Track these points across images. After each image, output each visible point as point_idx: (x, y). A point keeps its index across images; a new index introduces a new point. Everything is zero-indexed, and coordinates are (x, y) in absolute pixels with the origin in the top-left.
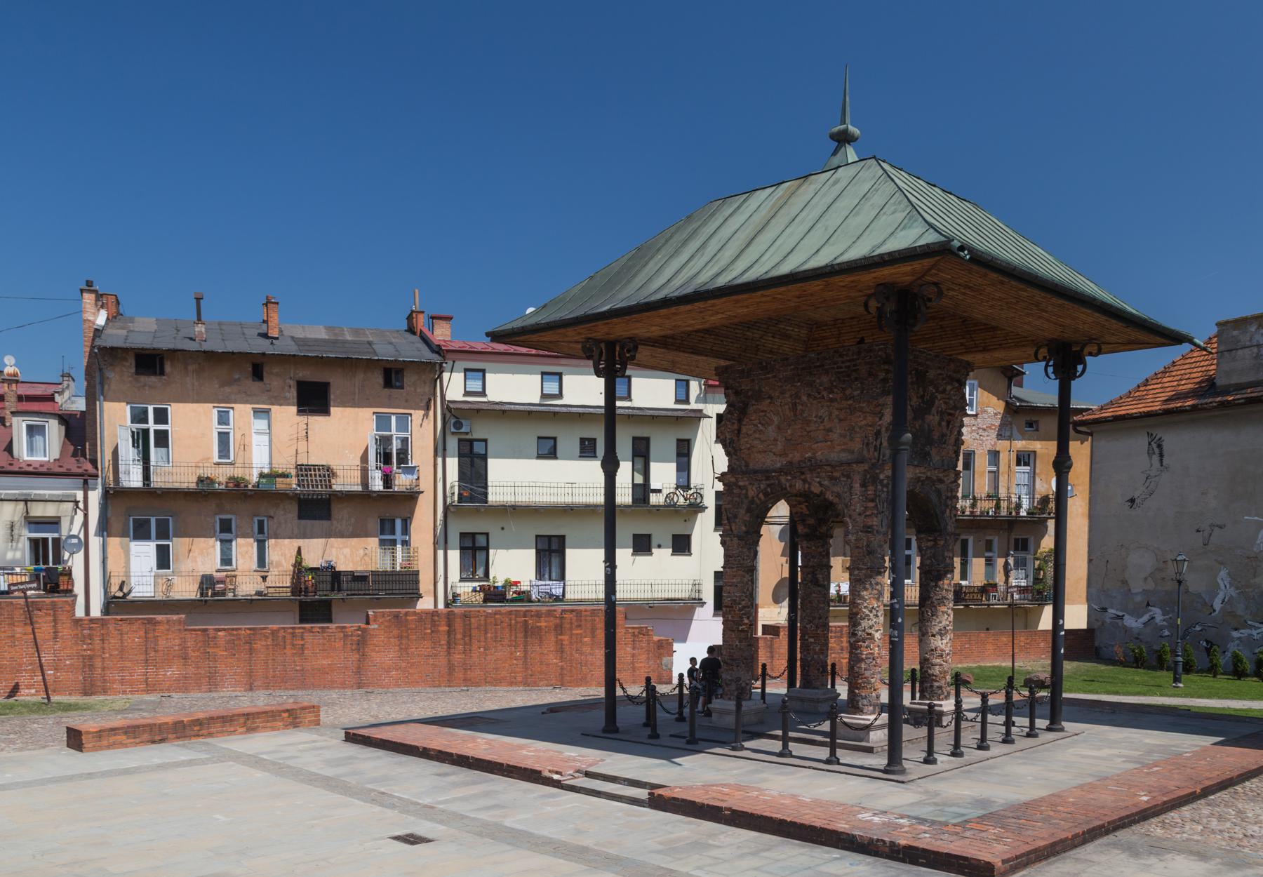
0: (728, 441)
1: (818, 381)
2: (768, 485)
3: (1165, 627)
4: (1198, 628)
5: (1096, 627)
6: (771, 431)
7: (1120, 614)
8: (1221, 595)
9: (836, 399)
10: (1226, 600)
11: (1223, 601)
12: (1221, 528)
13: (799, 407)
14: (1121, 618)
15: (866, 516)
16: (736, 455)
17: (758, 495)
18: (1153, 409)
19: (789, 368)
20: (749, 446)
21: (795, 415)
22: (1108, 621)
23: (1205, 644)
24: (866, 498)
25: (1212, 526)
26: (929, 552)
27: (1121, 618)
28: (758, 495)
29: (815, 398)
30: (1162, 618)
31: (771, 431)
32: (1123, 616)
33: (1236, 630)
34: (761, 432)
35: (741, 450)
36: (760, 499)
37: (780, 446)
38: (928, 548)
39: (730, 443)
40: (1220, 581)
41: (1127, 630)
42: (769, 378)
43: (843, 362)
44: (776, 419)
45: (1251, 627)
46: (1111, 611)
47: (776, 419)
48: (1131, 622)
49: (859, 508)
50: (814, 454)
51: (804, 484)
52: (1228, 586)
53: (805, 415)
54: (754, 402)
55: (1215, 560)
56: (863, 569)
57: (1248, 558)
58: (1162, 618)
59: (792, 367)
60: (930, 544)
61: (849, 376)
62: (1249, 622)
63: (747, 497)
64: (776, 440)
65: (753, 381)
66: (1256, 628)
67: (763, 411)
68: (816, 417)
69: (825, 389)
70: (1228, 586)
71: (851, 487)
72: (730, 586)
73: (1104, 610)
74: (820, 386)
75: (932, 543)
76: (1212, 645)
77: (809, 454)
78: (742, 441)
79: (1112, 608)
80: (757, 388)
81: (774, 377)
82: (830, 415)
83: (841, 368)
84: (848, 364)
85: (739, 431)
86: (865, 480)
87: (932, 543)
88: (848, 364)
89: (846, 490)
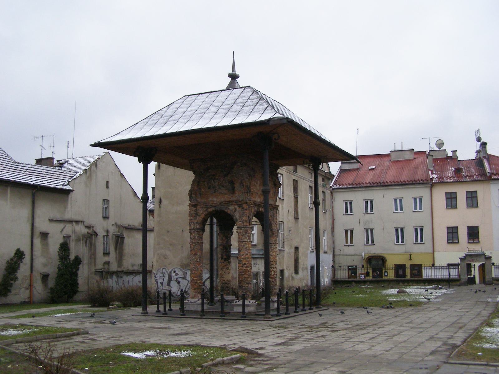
0: (248, 187)
28: (254, 212)
35: (251, 191)
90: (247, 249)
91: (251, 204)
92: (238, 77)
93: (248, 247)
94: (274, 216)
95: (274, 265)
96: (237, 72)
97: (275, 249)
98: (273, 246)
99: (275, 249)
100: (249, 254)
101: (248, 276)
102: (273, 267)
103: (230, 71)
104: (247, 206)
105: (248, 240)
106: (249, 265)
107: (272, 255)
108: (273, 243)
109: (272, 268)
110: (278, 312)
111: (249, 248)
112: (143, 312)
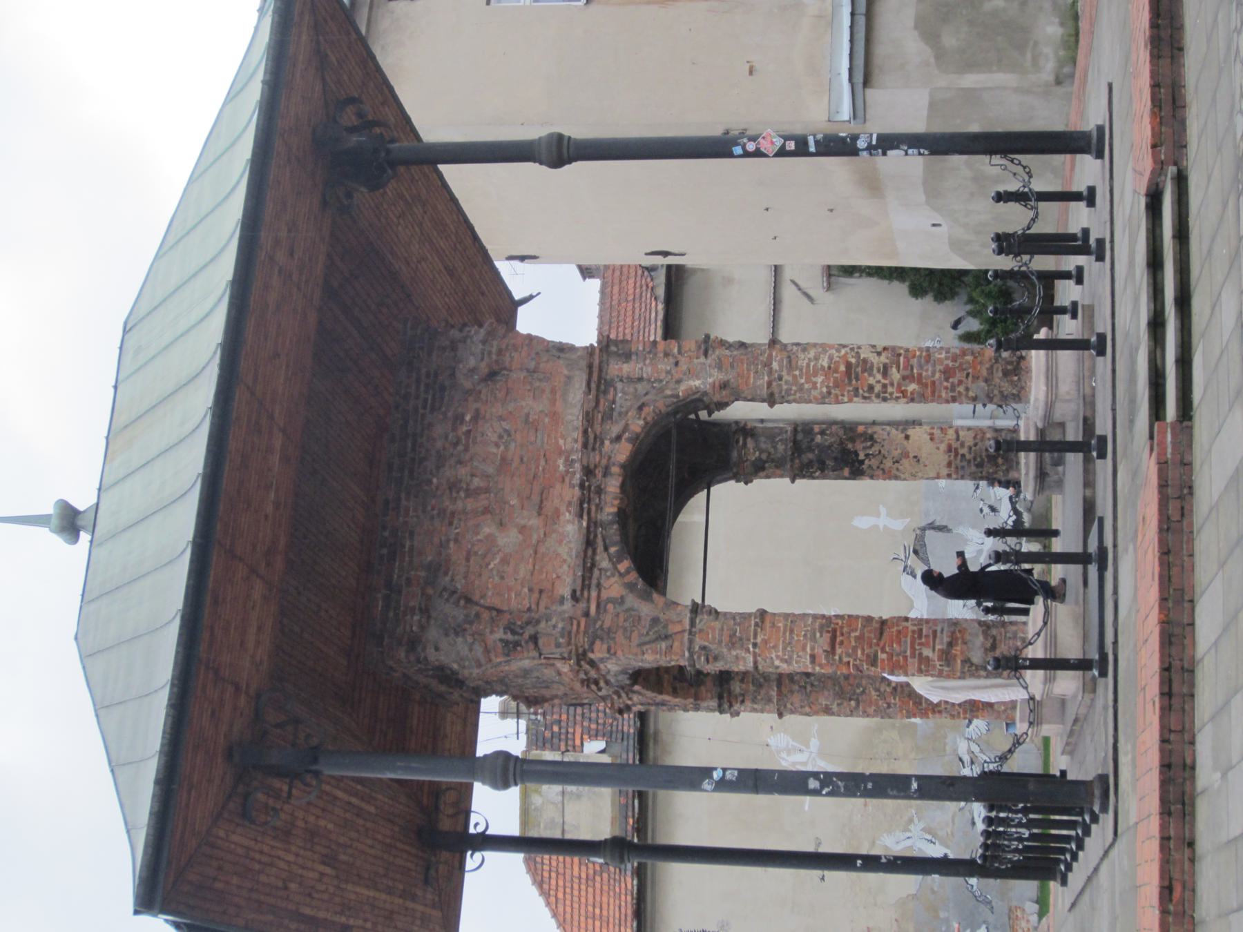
0: (510, 637)
1: (439, 444)
2: (606, 549)
6: (508, 539)
9: (477, 411)
10: (929, 837)
11: (932, 842)
12: (820, 843)
13: (477, 482)
15: (680, 352)
16: (538, 622)
17: (621, 575)
19: (404, 503)
20: (526, 590)
21: (487, 490)
24: (649, 352)
26: (763, 446)
29: (466, 449)
31: (508, 539)
34: (505, 561)
35: (529, 609)
36: (628, 572)
37: (534, 522)
38: (757, 448)
39: (514, 633)
42: (412, 548)
43: (417, 397)
44: (486, 530)
47: (486, 530)
50: (560, 452)
51: (611, 474)
52: (909, 834)
53: (491, 470)
54: (448, 579)
56: (770, 356)
59: (403, 495)
60: (750, 443)
61: (443, 389)
63: (622, 600)
64: (522, 529)
65: (409, 582)
67: (468, 560)
68: (497, 445)
69: (454, 429)
70: (909, 834)
71: (630, 380)
72: (792, 631)
74: (446, 437)
75: (749, 440)
77: (561, 462)
78: (514, 604)
80: (422, 574)
81: (412, 534)
82: (501, 418)
83: (426, 400)
84: (422, 388)
85: (490, 609)
86: (619, 355)
87: (749, 440)
88: (422, 388)
89: (631, 390)
90: (791, 658)
91: (587, 614)
93: (780, 654)
94: (640, 379)
95: (871, 381)
96: (49, 509)
97: (797, 373)
98: (783, 383)
99: (797, 373)
100: (813, 649)
101: (913, 656)
102: (885, 386)
104: (598, 643)
105: (748, 650)
106: (863, 650)
107: (825, 390)
108: (769, 384)
109: (890, 389)
111: (784, 649)
112: (1059, 880)
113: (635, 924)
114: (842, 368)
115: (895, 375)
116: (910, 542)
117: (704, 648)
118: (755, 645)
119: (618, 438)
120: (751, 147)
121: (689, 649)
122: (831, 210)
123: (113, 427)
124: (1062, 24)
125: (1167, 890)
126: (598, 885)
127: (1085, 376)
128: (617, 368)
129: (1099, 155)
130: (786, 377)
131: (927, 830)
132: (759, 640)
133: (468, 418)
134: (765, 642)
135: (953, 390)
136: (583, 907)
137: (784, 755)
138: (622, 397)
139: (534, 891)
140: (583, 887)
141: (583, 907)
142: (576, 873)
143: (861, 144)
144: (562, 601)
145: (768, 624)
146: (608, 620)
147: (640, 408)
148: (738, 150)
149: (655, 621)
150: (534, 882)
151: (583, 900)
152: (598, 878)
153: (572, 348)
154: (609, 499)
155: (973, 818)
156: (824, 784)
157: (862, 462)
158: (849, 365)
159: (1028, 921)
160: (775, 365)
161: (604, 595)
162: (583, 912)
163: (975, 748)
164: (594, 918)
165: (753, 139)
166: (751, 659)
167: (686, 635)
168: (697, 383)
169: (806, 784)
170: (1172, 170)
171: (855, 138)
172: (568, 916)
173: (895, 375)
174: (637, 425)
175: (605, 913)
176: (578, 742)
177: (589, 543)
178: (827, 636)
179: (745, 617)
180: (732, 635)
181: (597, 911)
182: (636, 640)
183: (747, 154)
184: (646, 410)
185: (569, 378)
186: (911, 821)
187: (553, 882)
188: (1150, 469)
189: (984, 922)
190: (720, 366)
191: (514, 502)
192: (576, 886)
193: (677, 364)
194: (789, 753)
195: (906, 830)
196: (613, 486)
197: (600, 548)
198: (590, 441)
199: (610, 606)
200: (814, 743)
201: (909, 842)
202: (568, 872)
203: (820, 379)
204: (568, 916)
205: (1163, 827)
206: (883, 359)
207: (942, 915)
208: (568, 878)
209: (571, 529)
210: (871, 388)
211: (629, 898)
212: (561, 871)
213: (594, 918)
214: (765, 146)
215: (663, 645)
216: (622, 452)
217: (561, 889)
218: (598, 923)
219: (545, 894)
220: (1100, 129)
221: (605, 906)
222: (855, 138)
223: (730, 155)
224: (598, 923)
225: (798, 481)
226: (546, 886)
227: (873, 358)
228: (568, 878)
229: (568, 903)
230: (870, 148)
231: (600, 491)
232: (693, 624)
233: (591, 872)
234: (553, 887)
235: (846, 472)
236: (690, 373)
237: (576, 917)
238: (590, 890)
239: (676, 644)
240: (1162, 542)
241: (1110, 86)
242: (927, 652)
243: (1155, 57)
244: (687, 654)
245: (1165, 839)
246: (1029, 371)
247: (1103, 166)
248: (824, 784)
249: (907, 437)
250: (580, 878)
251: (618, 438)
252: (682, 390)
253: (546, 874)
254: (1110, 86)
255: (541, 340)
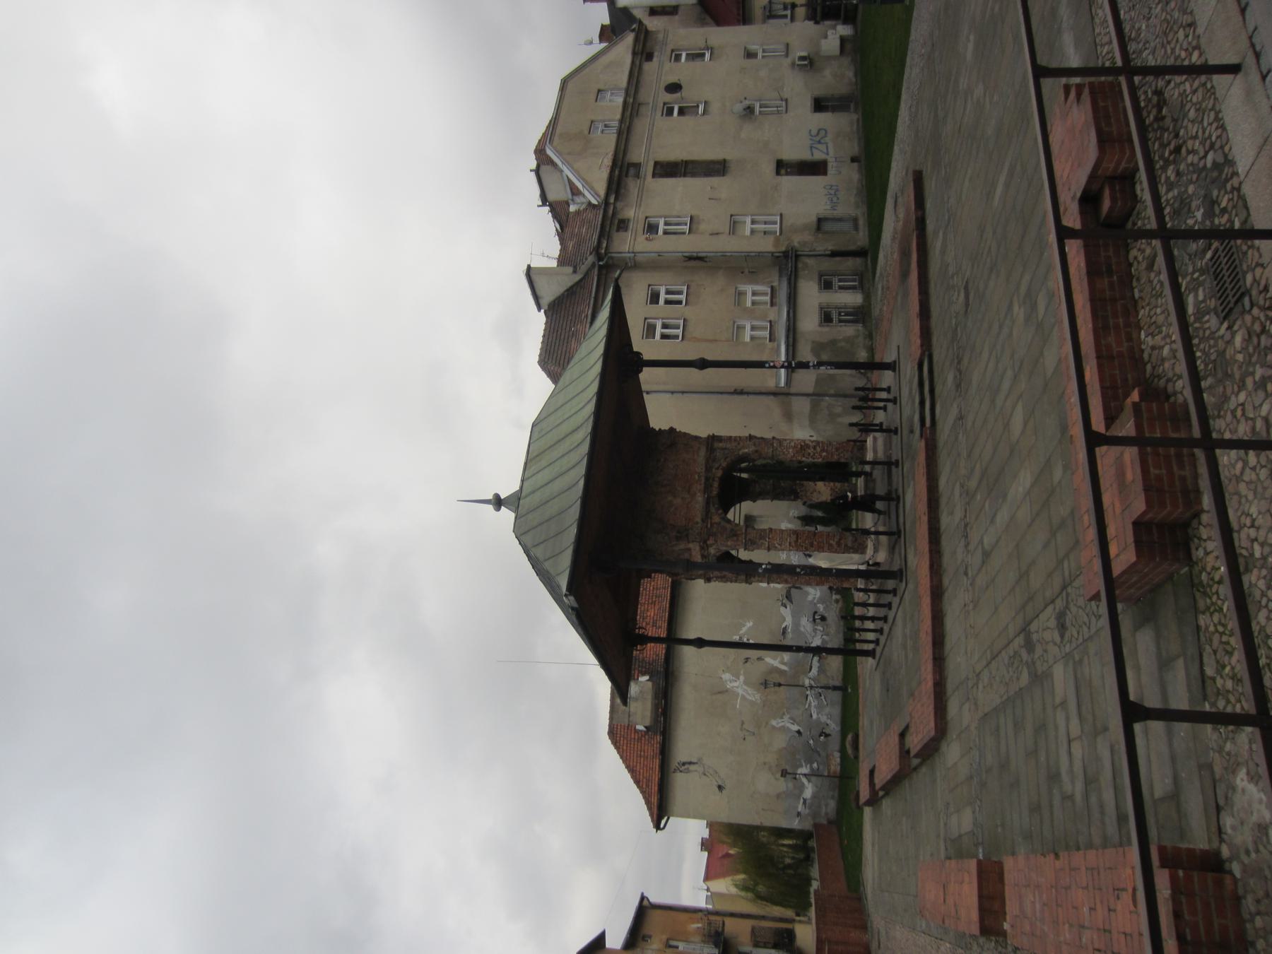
0: (678, 535)
2: (714, 506)
3: (811, 767)
4: (811, 742)
5: (812, 822)
7: (802, 801)
8: (789, 725)
14: (805, 801)
18: (657, 764)
22: (807, 811)
23: (822, 738)
25: (741, 730)
27: (805, 801)
30: (804, 768)
31: (678, 501)
32: (803, 798)
33: (811, 716)
40: (780, 725)
41: (814, 796)
45: (810, 705)
46: (799, 810)
48: (808, 792)
49: (734, 444)
55: (765, 727)
57: (764, 706)
58: (804, 768)
62: (807, 706)
63: (719, 524)
64: (682, 498)
66: (810, 702)
73: (799, 814)
76: (823, 732)
77: (697, 477)
79: (797, 807)
91: (707, 526)
92: (497, 497)
94: (725, 449)
95: (809, 451)
96: (490, 497)
103: (490, 507)
104: (711, 538)
108: (773, 451)
110: (892, 499)
113: (661, 757)
114: (799, 446)
115: (818, 449)
116: (784, 592)
117: (750, 540)
118: (769, 538)
119: (718, 468)
120: (772, 364)
121: (745, 539)
122: (771, 428)
123: (529, 458)
124: (867, 352)
125: (931, 566)
126: (643, 742)
127: (888, 445)
128: (716, 445)
129: (894, 370)
130: (779, 449)
131: (791, 718)
132: (770, 536)
133: (662, 460)
134: (773, 537)
135: (839, 455)
136: (635, 752)
137: (728, 683)
138: (718, 454)
139: (612, 747)
140: (636, 743)
141: (635, 752)
142: (633, 737)
143: (811, 364)
144: (697, 523)
145: (773, 532)
146: (715, 530)
147: (725, 459)
148: (767, 365)
149: (732, 530)
150: (612, 743)
151: (636, 749)
152: (643, 738)
153: (700, 438)
154: (714, 489)
155: (811, 714)
156: (802, 570)
157: (798, 493)
158: (801, 445)
159: (835, 761)
160: (775, 445)
161: (713, 521)
162: (635, 755)
163: (812, 683)
164: (641, 757)
165: (772, 362)
166: (767, 543)
167: (744, 535)
168: (746, 450)
169: (795, 570)
170: (927, 353)
171: (809, 362)
172: (628, 757)
173: (818, 449)
174: (724, 464)
175: (646, 754)
176: (636, 677)
177: (708, 503)
178: (795, 536)
179: (765, 530)
180: (761, 535)
181: (642, 753)
182: (725, 536)
183: (770, 367)
184: (728, 460)
185: (699, 448)
186: (784, 714)
187: (622, 742)
188: (923, 444)
189: (816, 761)
190: (755, 445)
191: (679, 489)
192: (632, 743)
193: (739, 444)
194: (731, 682)
195: (782, 718)
196: (716, 485)
197: (711, 505)
198: (708, 469)
199: (715, 525)
200: (742, 678)
201: (783, 724)
202: (629, 736)
203: (791, 450)
204: (628, 757)
205: (930, 547)
206: (814, 444)
207: (798, 757)
208: (629, 739)
209: (700, 498)
210: (809, 454)
211: (658, 745)
212: (626, 736)
213: (641, 757)
214: (777, 364)
215: (735, 538)
216: (719, 473)
217: (625, 745)
218: (642, 759)
219: (617, 747)
220: (895, 362)
221: (646, 751)
222: (809, 362)
223: (764, 367)
224: (642, 759)
225: (774, 502)
226: (618, 744)
227: (811, 444)
228: (629, 739)
229: (628, 751)
230: (814, 366)
231: (711, 486)
232: (746, 530)
233: (640, 735)
234: (622, 744)
235: (792, 497)
236: (743, 447)
237: (632, 758)
238: (639, 744)
239: (740, 539)
240: (927, 463)
241: (898, 347)
242: (831, 542)
243: (921, 320)
244: (744, 541)
245: (931, 551)
246: (866, 449)
247: (895, 375)
248: (802, 570)
249: (816, 485)
250: (634, 739)
251: (718, 468)
252: (741, 453)
253: (618, 739)
254: (898, 347)
255: (689, 434)
